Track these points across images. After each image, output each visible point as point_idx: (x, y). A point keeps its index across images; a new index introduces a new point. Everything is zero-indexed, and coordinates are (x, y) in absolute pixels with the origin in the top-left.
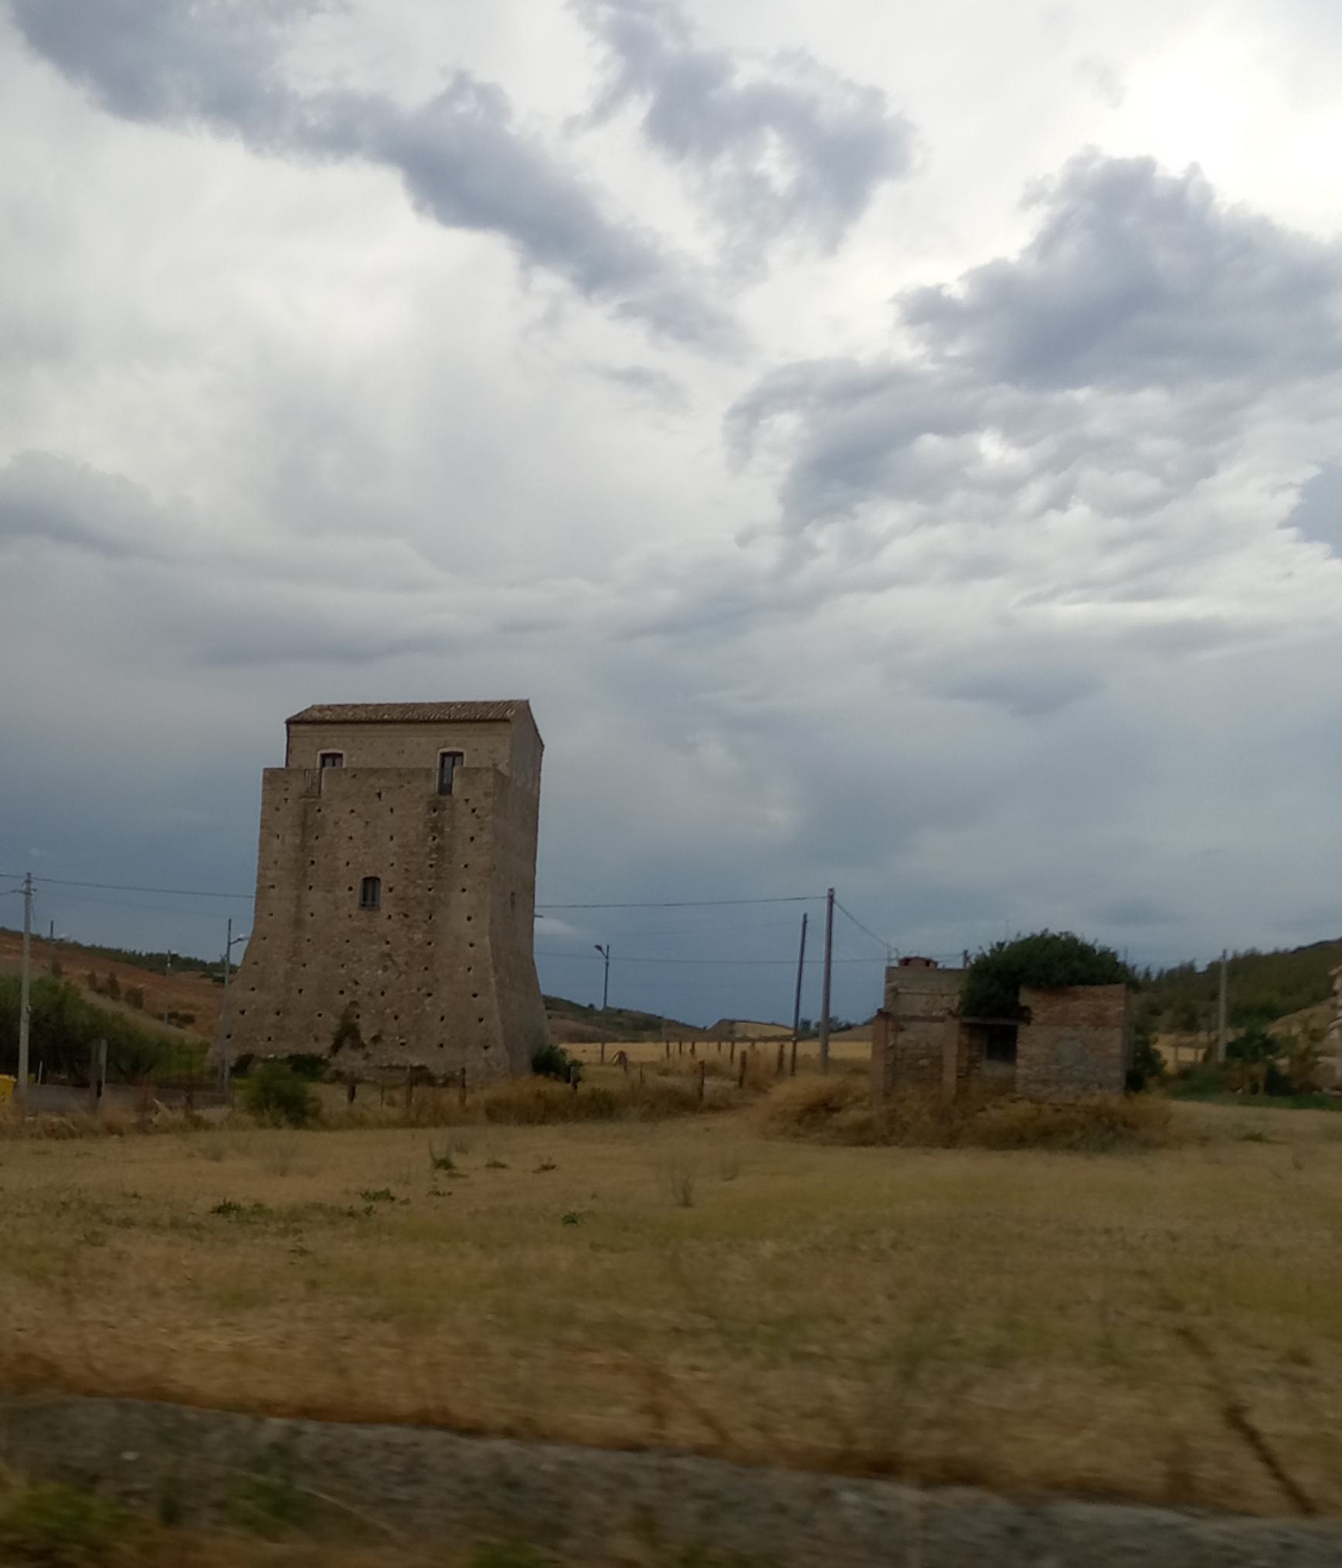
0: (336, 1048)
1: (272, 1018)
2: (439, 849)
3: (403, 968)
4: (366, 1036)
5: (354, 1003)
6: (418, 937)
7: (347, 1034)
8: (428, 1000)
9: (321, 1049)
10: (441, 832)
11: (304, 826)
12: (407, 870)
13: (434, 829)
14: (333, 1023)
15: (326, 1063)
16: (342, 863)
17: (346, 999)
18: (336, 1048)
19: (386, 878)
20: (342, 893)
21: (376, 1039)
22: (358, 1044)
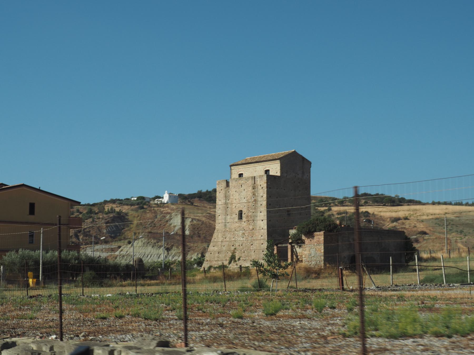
0: (230, 263)
1: (217, 255)
2: (255, 200)
3: (247, 237)
4: (237, 259)
5: (235, 249)
6: (251, 227)
7: (233, 258)
8: (252, 246)
9: (226, 263)
10: (255, 195)
11: (226, 197)
12: (248, 208)
13: (254, 194)
14: (230, 254)
15: (227, 267)
16: (234, 207)
17: (233, 248)
18: (230, 263)
19: (245, 211)
20: (234, 216)
21: (239, 259)
22: (235, 261)
